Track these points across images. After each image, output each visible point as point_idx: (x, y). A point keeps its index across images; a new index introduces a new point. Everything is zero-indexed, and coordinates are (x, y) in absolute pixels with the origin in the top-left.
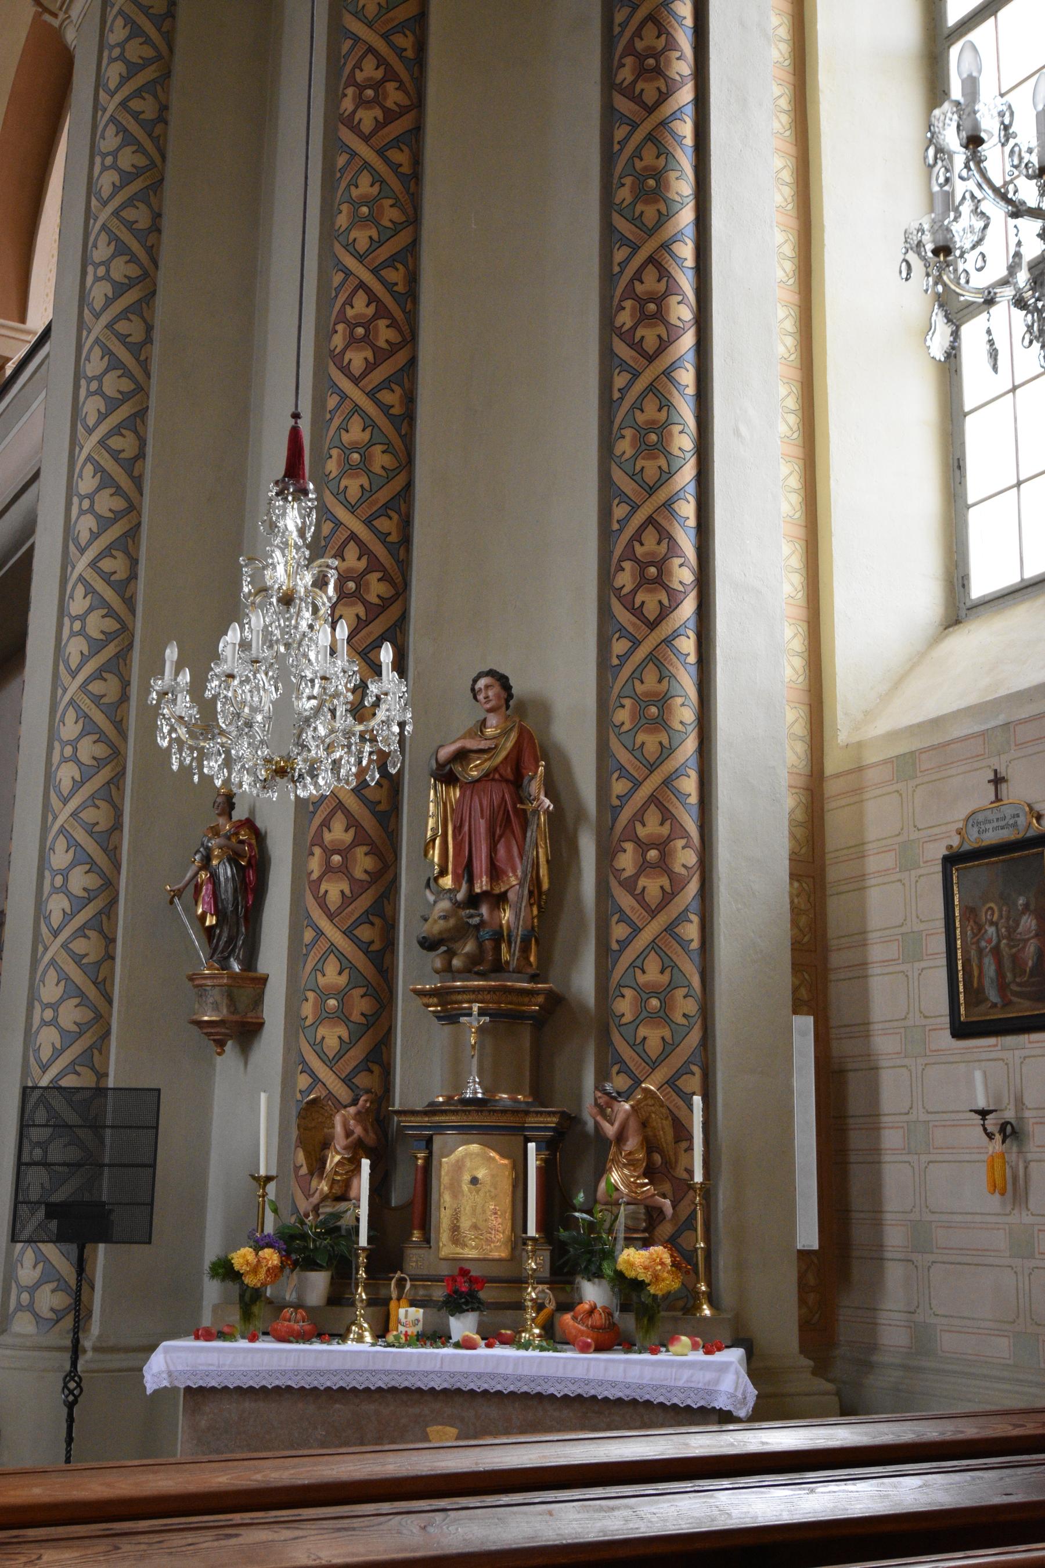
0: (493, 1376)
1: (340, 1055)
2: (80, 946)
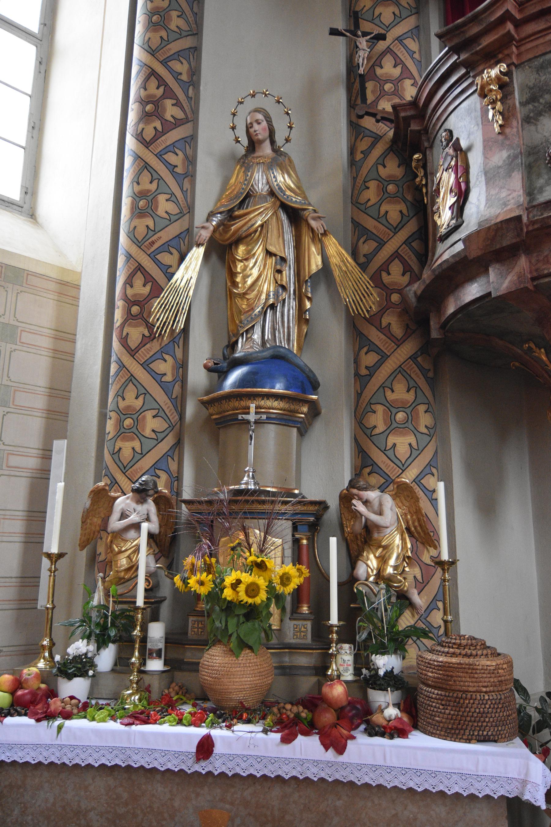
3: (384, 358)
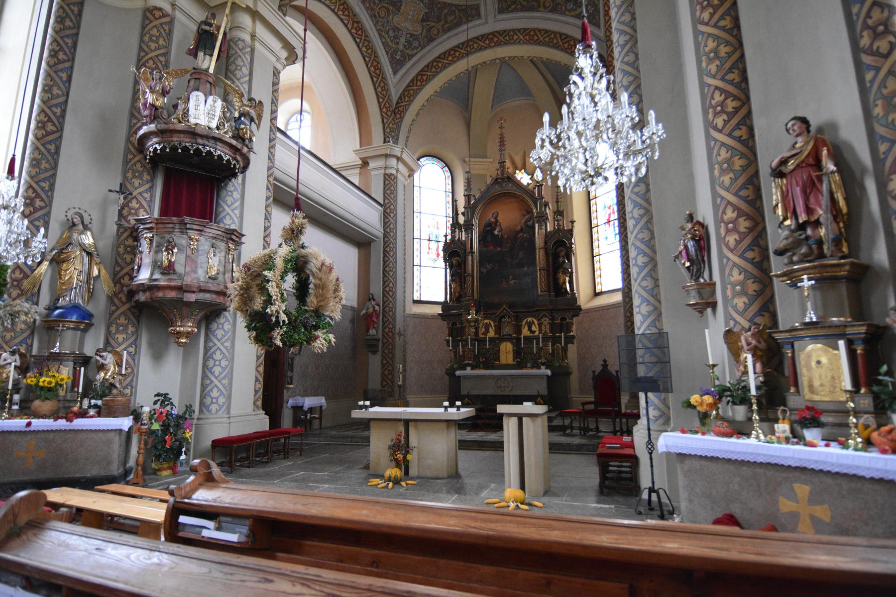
0: (825, 463)
1: (745, 310)
2: (644, 284)
3: (118, 308)
